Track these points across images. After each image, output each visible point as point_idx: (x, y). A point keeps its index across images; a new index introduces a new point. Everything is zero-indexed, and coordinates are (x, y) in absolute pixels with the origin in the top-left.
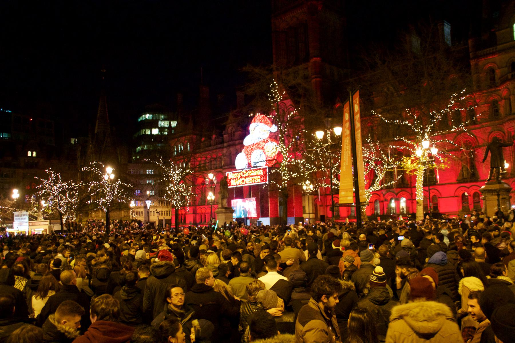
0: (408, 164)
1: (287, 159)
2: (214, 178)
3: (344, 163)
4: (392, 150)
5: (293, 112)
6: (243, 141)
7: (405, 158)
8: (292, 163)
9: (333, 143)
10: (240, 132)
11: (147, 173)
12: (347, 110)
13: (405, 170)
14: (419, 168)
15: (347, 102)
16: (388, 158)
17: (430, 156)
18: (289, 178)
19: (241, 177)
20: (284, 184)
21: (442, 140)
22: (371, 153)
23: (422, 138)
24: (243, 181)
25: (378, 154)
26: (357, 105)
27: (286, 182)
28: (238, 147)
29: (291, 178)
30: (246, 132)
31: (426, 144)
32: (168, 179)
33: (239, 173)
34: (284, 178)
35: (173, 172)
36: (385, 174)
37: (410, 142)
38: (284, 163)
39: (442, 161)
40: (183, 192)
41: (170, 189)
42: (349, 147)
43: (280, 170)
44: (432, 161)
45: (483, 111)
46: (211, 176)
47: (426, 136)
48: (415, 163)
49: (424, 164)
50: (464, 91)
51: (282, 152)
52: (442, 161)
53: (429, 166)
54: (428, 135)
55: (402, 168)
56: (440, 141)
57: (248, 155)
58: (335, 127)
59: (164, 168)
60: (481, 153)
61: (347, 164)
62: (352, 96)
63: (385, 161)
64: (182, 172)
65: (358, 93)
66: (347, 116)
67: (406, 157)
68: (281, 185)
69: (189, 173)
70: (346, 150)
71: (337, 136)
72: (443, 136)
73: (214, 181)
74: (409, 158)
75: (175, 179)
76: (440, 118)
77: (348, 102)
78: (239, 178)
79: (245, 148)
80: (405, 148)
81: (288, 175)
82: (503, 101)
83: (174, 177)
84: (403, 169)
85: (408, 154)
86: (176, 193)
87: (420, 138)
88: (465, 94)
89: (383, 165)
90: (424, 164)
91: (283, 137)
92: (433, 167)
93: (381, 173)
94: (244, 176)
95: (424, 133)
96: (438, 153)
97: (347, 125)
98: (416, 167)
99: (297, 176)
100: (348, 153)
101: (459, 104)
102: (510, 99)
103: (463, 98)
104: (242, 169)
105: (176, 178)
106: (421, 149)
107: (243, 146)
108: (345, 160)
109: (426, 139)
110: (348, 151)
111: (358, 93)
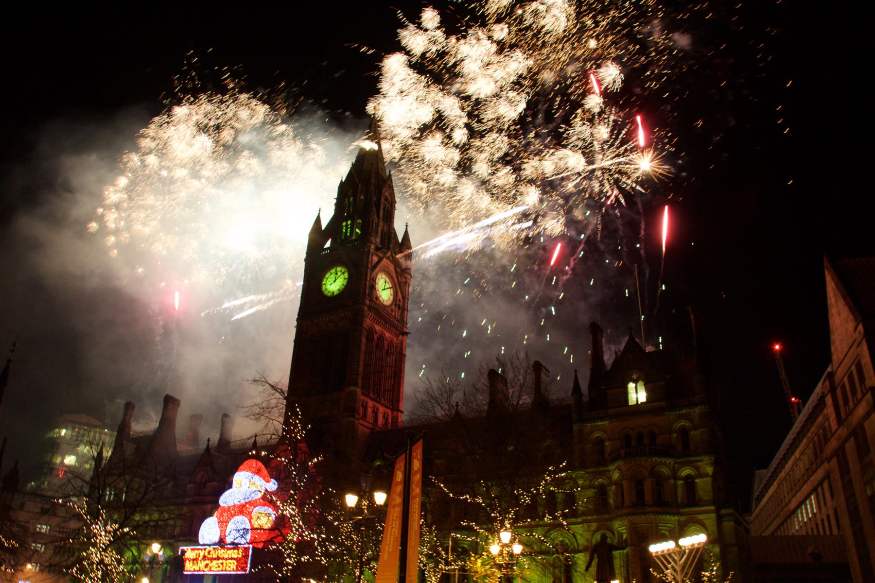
0: (477, 565)
2: (161, 553)
3: (387, 547)
4: (455, 540)
5: (318, 459)
6: (219, 498)
7: (473, 555)
8: (306, 538)
9: (370, 517)
10: (215, 483)
12: (401, 466)
13: (471, 574)
14: (493, 574)
16: (447, 553)
17: (511, 555)
18: (295, 562)
19: (204, 558)
20: (286, 571)
21: (528, 534)
22: (422, 542)
23: (501, 528)
24: (206, 566)
25: (434, 548)
26: (419, 460)
27: (290, 567)
28: (209, 507)
29: (299, 562)
30: (228, 485)
31: (506, 536)
32: (89, 539)
33: (201, 550)
34: (288, 560)
36: (439, 578)
37: (482, 530)
38: (293, 537)
39: (526, 567)
40: (110, 565)
41: (88, 558)
42: (397, 523)
43: (283, 547)
44: (513, 565)
45: (588, 496)
46: (156, 548)
47: (508, 526)
48: (487, 564)
49: (500, 567)
50: (564, 464)
52: (526, 567)
53: (508, 572)
54: (509, 523)
55: (466, 571)
56: (526, 535)
57: (223, 523)
60: (581, 559)
61: (391, 550)
62: (411, 446)
63: (442, 558)
64: (115, 531)
65: (420, 444)
66: (399, 476)
67: (476, 553)
68: (281, 572)
69: (128, 533)
70: (392, 528)
71: (377, 505)
72: (530, 528)
73: (159, 557)
74: (479, 556)
77: (404, 455)
78: (200, 558)
79: (219, 510)
80: (474, 539)
81: (294, 556)
82: (614, 487)
83: (101, 536)
84: (468, 573)
85: (477, 549)
86: (97, 568)
87: (497, 527)
88: (564, 470)
89: (437, 564)
90: (500, 567)
91: (295, 494)
92: (514, 573)
93: (435, 576)
94: (211, 556)
96: (522, 554)
97: (399, 489)
98: (488, 572)
99: (308, 560)
100: (394, 533)
102: (622, 485)
103: (562, 475)
104: (209, 545)
105: (104, 539)
106: (498, 544)
107: (216, 505)
108: (388, 542)
109: (506, 530)
111: (420, 444)
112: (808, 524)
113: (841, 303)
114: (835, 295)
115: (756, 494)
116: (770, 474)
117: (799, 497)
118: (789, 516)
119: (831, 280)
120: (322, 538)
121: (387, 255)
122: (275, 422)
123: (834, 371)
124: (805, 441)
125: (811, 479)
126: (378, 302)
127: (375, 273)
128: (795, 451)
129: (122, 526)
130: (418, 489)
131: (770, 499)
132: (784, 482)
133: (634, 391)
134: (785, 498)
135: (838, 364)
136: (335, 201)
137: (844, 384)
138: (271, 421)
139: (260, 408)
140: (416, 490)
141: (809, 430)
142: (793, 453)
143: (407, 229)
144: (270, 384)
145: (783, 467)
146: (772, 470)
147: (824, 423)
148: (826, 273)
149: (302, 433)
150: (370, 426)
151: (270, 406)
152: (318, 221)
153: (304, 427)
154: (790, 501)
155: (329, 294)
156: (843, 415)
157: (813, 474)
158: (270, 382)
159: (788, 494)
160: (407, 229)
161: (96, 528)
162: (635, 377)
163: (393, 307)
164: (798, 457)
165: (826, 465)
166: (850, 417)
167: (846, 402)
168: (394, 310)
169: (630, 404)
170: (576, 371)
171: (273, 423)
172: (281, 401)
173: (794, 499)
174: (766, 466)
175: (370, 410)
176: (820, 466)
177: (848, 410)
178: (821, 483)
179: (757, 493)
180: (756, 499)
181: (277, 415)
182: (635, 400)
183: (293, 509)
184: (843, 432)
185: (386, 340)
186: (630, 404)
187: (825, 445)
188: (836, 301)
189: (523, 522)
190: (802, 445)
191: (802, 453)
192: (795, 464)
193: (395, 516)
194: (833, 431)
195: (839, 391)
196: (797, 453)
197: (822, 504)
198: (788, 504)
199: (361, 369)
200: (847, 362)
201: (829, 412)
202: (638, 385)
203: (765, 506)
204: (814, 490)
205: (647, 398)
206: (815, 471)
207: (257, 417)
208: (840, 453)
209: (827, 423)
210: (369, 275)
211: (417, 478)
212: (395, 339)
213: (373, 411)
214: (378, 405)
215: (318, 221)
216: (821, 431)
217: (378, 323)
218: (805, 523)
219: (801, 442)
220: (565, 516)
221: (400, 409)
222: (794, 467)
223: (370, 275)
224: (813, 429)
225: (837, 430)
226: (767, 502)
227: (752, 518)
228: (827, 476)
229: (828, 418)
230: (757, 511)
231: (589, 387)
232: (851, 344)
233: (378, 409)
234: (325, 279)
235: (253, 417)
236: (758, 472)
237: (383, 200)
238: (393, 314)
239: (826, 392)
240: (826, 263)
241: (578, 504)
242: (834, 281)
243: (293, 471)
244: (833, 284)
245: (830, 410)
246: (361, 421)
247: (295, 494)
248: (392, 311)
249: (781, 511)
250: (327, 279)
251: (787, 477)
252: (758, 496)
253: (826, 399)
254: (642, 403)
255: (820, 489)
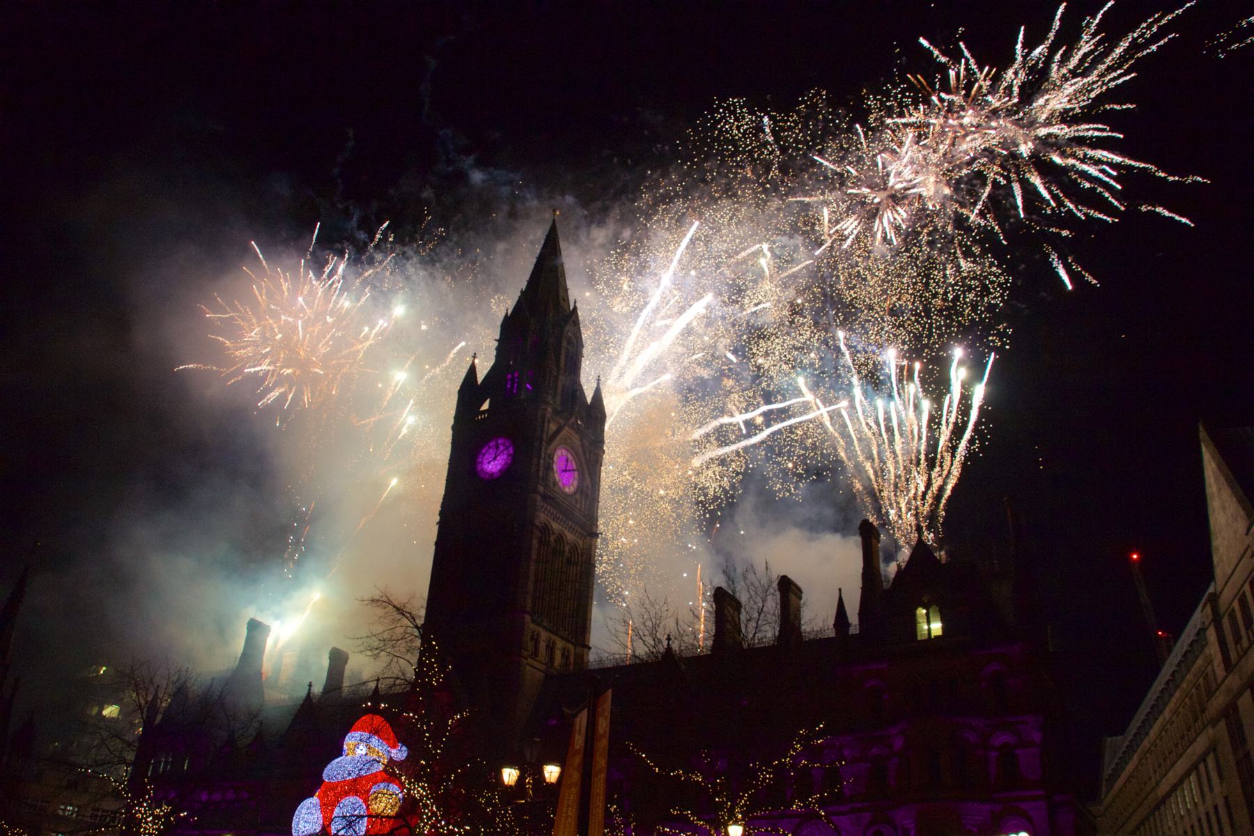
1: (429, 818)
9: (536, 800)
11: (61, 813)
15: (583, 709)
23: (730, 819)
35: (146, 813)
42: (574, 810)
51: (421, 800)
54: (741, 813)
56: (766, 830)
57: (327, 807)
58: (547, 765)
59: (128, 798)
64: (167, 815)
66: (579, 741)
70: (567, 818)
71: (548, 783)
75: (145, 829)
76: (769, 778)
79: (323, 787)
83: (147, 823)
87: (723, 818)
95: (732, 808)
97: (577, 760)
101: (810, 752)
109: (736, 822)
110: (570, 819)
112: (1187, 818)
113: (1227, 493)
114: (1216, 479)
115: (1107, 771)
116: (1127, 743)
117: (1172, 777)
118: (1157, 807)
119: (1211, 460)
120: (465, 830)
121: (570, 422)
122: (401, 661)
123: (1218, 593)
124: (1177, 694)
125: (1189, 751)
126: (556, 489)
127: (551, 447)
128: (1164, 709)
129: (175, 812)
130: (604, 761)
131: (1128, 780)
132: (1148, 755)
133: (925, 620)
134: (1150, 778)
135: (1223, 584)
136: (496, 344)
137: (1233, 610)
138: (395, 659)
139: (380, 640)
140: (601, 762)
141: (1183, 678)
142: (1161, 712)
143: (598, 384)
144: (394, 606)
145: (1147, 734)
146: (1130, 737)
147: (1206, 668)
148: (1204, 449)
149: (440, 677)
150: (542, 667)
151: (395, 637)
152: (472, 370)
153: (442, 668)
154: (1157, 784)
155: (487, 477)
156: (1233, 656)
157: (1190, 745)
158: (396, 603)
159: (1155, 772)
160: (598, 384)
161: (141, 811)
162: (925, 599)
163: (578, 496)
164: (1167, 719)
165: (1210, 731)
166: (1244, 659)
167: (1238, 639)
168: (579, 501)
169: (919, 638)
170: (840, 590)
171: (398, 662)
172: (409, 630)
173: (1164, 780)
174: (1120, 730)
175: (543, 645)
176: (1201, 732)
177: (1239, 650)
178: (1203, 759)
179: (1109, 772)
180: (1107, 780)
181: (404, 650)
182: (926, 632)
183: (423, 788)
184: (1234, 681)
185: (568, 544)
186: (919, 638)
187: (1207, 702)
188: (1219, 490)
189: (761, 810)
190: (1174, 700)
191: (1175, 712)
192: (1163, 728)
193: (570, 797)
194: (1219, 680)
195: (1226, 622)
196: (1167, 713)
197: (1206, 790)
198: (1154, 788)
199: (531, 587)
200: (1239, 577)
201: (1212, 652)
202: (931, 611)
203: (1121, 791)
204: (1194, 767)
205: (944, 629)
206: (1195, 740)
207: (376, 652)
208: (1230, 713)
209: (1210, 667)
210: (543, 450)
211: (603, 744)
212: (581, 542)
213: (548, 646)
214: (553, 637)
215: (472, 370)
216: (1201, 680)
217: (556, 519)
218: (1182, 817)
219: (1171, 695)
220: (822, 803)
221: (587, 643)
222: (1163, 733)
223: (546, 450)
224: (1189, 677)
225: (1226, 677)
226: (1125, 785)
227: (1102, 808)
228: (1213, 748)
229: (1211, 661)
230: (1109, 798)
231: (860, 614)
232: (1242, 552)
233: (554, 643)
234: (481, 456)
235: (369, 653)
236: (1109, 739)
237: (564, 343)
238: (578, 506)
239: (1207, 623)
240: (1203, 434)
241: (841, 784)
242: (1213, 458)
243: (425, 731)
244: (1214, 465)
245: (1213, 649)
246: (530, 661)
247: (428, 765)
248: (577, 502)
249: (1145, 799)
250: (484, 455)
251: (1153, 748)
252: (1110, 775)
253: (1208, 633)
254: (936, 637)
255: (1202, 767)
